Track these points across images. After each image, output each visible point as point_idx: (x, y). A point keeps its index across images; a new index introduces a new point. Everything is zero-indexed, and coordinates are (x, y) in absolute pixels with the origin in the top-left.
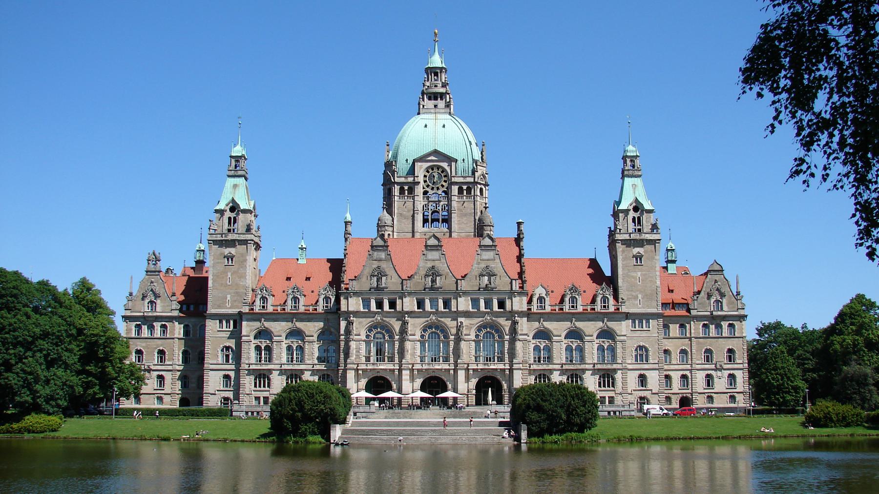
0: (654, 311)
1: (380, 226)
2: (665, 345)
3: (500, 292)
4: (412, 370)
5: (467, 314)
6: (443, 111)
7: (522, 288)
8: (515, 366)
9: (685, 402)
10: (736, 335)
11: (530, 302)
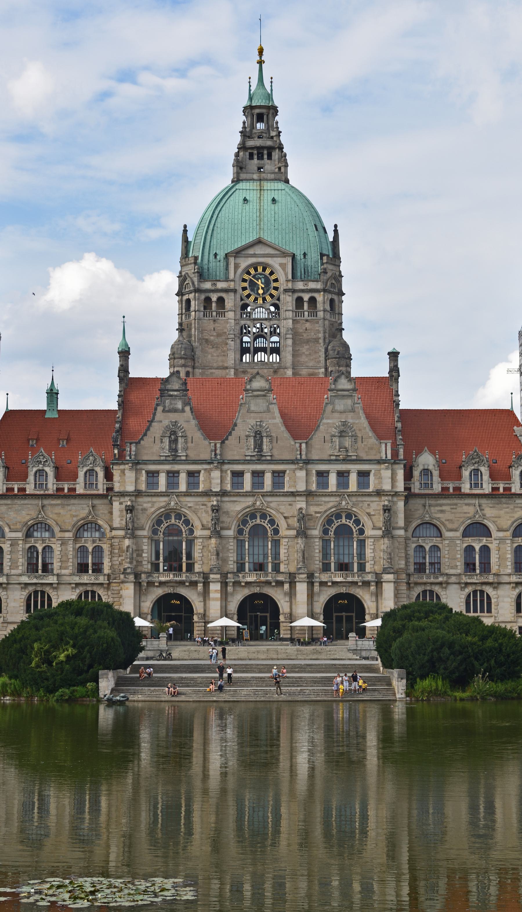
5: (308, 494)
6: (272, 176)
7: (395, 454)
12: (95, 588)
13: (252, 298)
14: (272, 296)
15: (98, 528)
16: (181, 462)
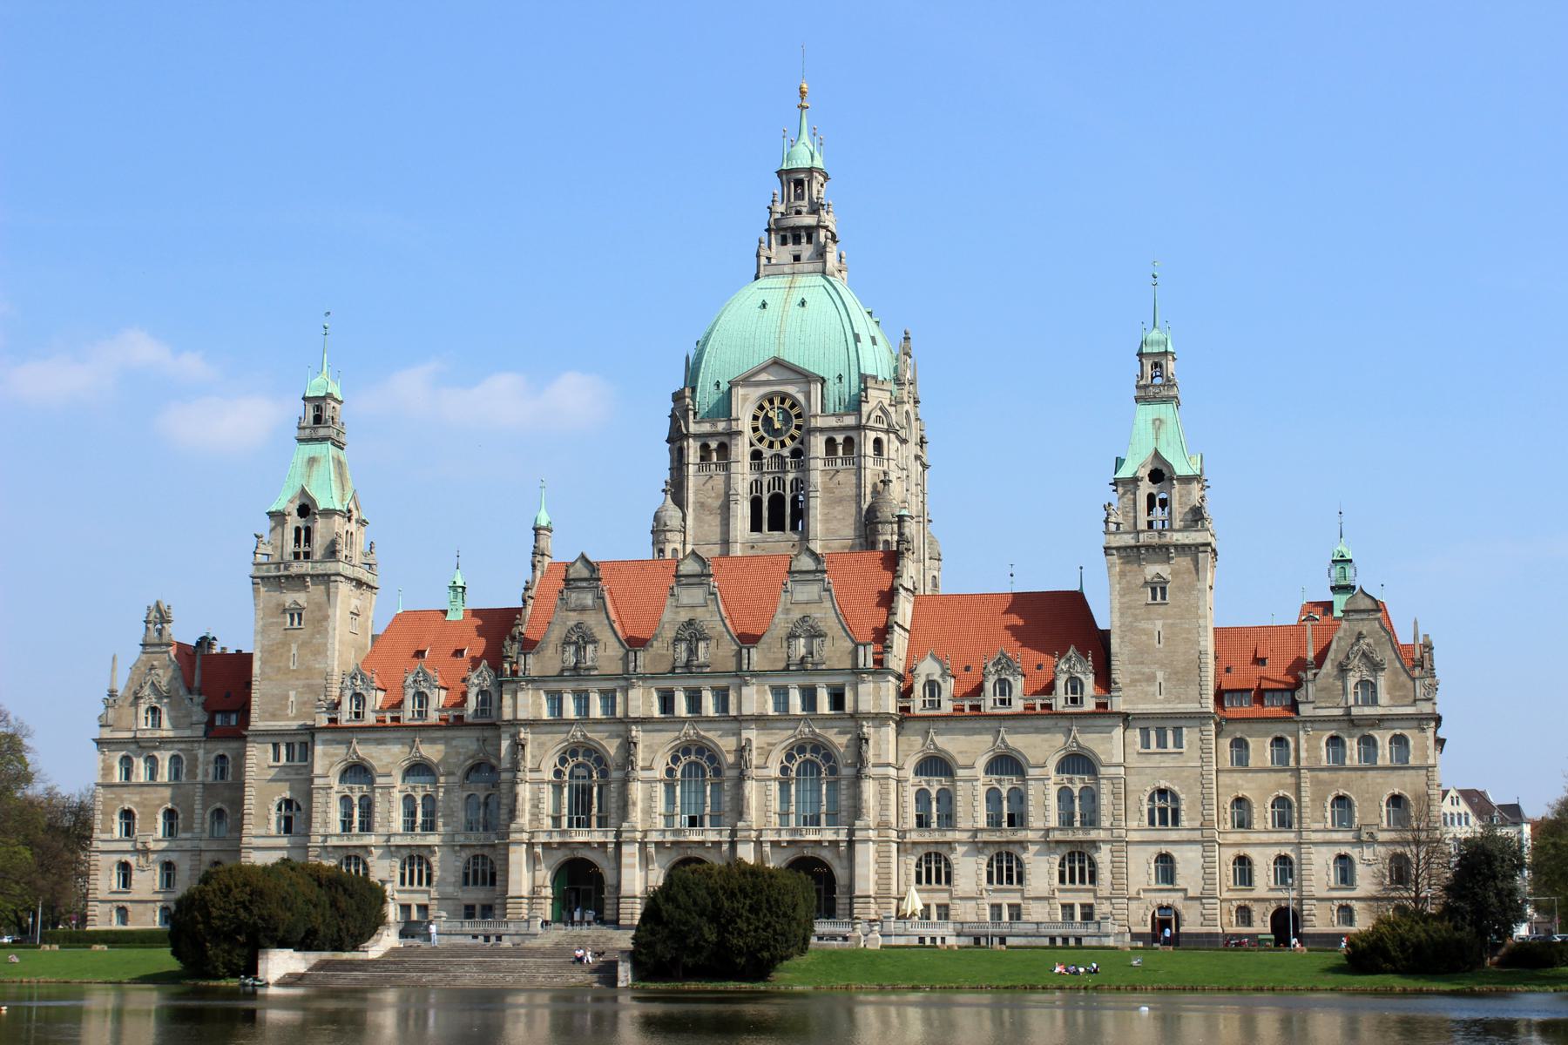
0: (1193, 707)
1: (659, 531)
2: (1237, 788)
3: (715, 674)
4: (643, 845)
5: (760, 720)
6: (810, 267)
7: (879, 662)
8: (859, 835)
9: (1285, 922)
10: (1412, 761)
11: (906, 693)
12: (486, 851)
13: (766, 442)
14: (793, 438)
15: (493, 769)
16: (589, 678)
